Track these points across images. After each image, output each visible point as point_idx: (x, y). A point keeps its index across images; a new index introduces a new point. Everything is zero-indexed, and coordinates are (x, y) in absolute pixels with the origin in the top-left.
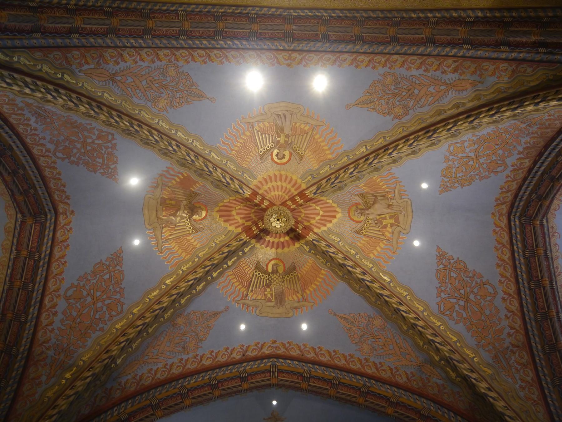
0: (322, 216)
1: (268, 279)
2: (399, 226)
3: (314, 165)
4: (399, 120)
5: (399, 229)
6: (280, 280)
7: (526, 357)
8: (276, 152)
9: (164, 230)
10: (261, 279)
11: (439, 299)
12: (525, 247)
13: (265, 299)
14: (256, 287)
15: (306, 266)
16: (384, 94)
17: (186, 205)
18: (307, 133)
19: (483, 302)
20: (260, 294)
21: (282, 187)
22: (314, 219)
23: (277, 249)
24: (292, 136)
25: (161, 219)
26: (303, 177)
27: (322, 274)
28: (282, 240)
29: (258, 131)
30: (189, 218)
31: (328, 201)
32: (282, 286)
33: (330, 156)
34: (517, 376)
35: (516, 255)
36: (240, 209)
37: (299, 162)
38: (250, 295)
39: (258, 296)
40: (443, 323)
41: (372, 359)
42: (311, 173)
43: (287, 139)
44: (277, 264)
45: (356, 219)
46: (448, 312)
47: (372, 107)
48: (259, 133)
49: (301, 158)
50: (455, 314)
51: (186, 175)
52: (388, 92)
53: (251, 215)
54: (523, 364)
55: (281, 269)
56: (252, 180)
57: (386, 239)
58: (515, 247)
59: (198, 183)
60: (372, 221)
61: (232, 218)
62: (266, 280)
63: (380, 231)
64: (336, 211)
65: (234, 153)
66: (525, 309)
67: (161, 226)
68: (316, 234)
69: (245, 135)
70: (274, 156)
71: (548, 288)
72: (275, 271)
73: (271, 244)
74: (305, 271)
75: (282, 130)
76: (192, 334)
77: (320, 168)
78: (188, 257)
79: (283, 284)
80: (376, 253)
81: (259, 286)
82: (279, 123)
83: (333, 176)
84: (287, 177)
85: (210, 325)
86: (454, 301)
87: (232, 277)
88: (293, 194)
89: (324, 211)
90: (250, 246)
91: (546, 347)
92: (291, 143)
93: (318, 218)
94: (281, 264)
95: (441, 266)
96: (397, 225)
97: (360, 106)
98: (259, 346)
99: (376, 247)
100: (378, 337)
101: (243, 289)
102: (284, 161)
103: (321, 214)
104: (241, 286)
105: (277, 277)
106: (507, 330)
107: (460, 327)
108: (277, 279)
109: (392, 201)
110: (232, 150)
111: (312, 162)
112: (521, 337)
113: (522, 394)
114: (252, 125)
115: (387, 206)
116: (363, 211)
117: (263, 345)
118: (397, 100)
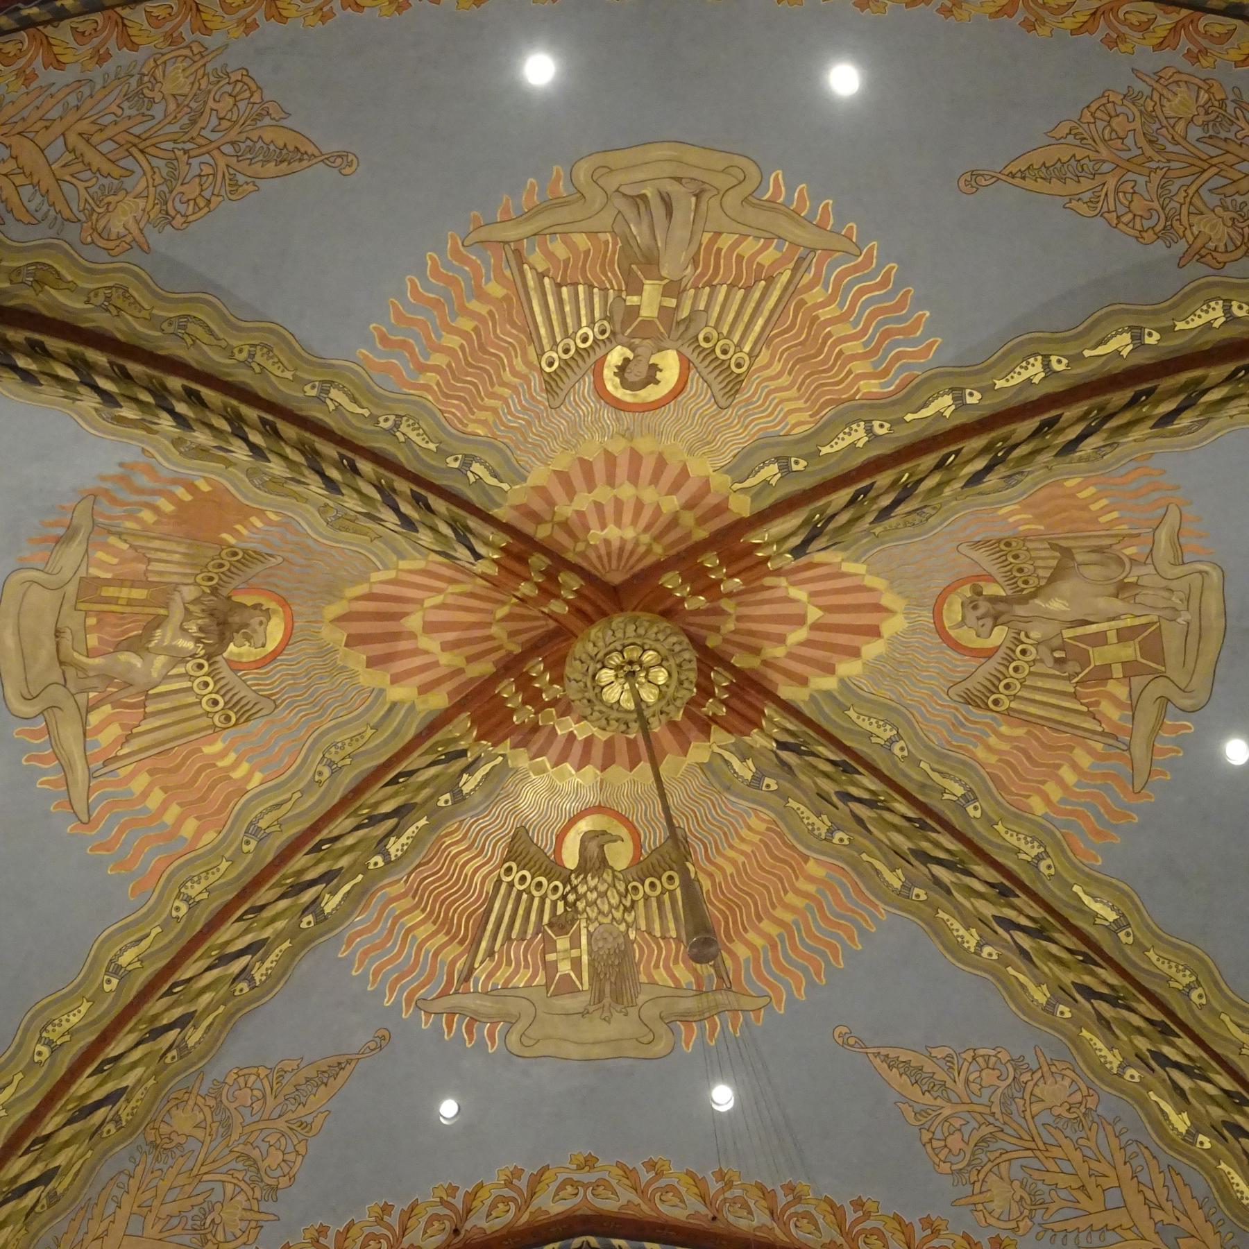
0: (816, 627)
1: (564, 897)
3: (792, 419)
4: (1212, 271)
5: (1159, 688)
6: (615, 901)
8: (616, 356)
9: (94, 719)
10: (532, 898)
13: (547, 986)
14: (508, 938)
15: (736, 842)
16: (1149, 152)
17: (196, 601)
18: (770, 280)
20: (527, 966)
21: (639, 506)
22: (781, 639)
23: (603, 768)
24: (697, 288)
25: (78, 667)
26: (741, 466)
27: (811, 879)
29: (541, 276)
30: (208, 657)
31: (848, 567)
32: (623, 927)
33: (871, 387)
36: (443, 606)
37: (723, 403)
38: (481, 972)
39: (516, 971)
42: (778, 451)
43: (672, 303)
44: (604, 833)
45: (967, 637)
47: (1087, 196)
48: (546, 280)
49: (734, 384)
51: (205, 487)
52: (1170, 147)
53: (494, 630)
55: (620, 856)
56: (505, 486)
57: (1103, 734)
59: (261, 513)
60: (1042, 648)
61: (403, 645)
62: (554, 904)
63: (1075, 696)
64: (878, 608)
65: (431, 378)
67: (82, 699)
68: (788, 708)
69: (480, 295)
70: (608, 373)
72: (594, 863)
73: (577, 750)
74: (734, 862)
75: (651, 262)
76: (234, 1165)
77: (824, 432)
78: (209, 837)
79: (630, 918)
80: (1055, 793)
81: (524, 931)
82: (639, 231)
83: (883, 479)
84: (661, 464)
85: (309, 1119)
87: (407, 903)
88: (689, 534)
89: (827, 609)
90: (488, 767)
92: (690, 319)
93: (797, 635)
94: (623, 832)
96: (1151, 671)
97: (1029, 183)
98: (523, 1184)
99: (1058, 767)
100: (1056, 1152)
101: (453, 951)
102: (651, 393)
103: (810, 620)
104: (442, 938)
105: (602, 888)
108: (603, 895)
109: (1137, 571)
110: (423, 369)
111: (788, 406)
114: (518, 253)
115: (1112, 589)
116: (1001, 607)
117: (536, 1180)
118: (1210, 185)
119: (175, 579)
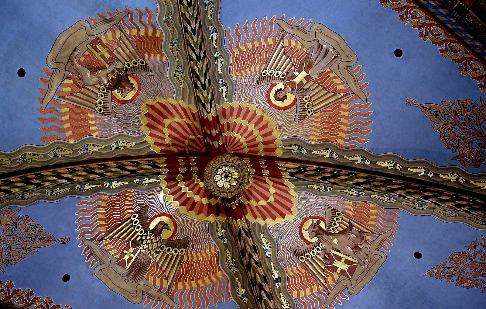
0: (269, 203)
1: (142, 236)
2: (349, 279)
3: (312, 137)
4: (461, 165)
5: (347, 282)
6: (154, 247)
8: (280, 86)
9: (66, 81)
10: (134, 230)
13: (118, 260)
14: (119, 237)
15: (203, 252)
16: (467, 123)
17: (119, 70)
18: (336, 94)
20: (117, 250)
21: (251, 133)
22: (258, 201)
23: (180, 205)
24: (315, 83)
25: (73, 63)
26: (286, 142)
27: (216, 277)
28: (197, 198)
29: (283, 47)
30: (108, 89)
31: (292, 192)
32: (151, 257)
33: (340, 141)
36: (179, 124)
37: (296, 120)
38: (105, 242)
39: (113, 249)
42: (301, 144)
43: (305, 82)
44: (166, 225)
45: (306, 234)
47: (440, 125)
48: (283, 49)
49: (304, 117)
51: (158, 35)
52: (474, 125)
53: (186, 141)
55: (166, 235)
56: (226, 100)
57: (324, 286)
59: (162, 56)
60: (323, 251)
61: (160, 127)
62: (138, 236)
63: (323, 270)
64: (289, 210)
65: (237, 52)
67: (67, 73)
68: (247, 222)
69: (266, 39)
70: (274, 89)
72: (157, 232)
73: (179, 194)
74: (198, 258)
75: (309, 66)
76: (5, 245)
77: (318, 147)
78: (72, 140)
79: (155, 256)
81: (124, 238)
83: (328, 169)
84: (266, 126)
85: (32, 249)
87: (104, 204)
88: (258, 152)
89: (275, 200)
90: (154, 180)
92: (306, 90)
93: (263, 203)
94: (172, 228)
96: (348, 277)
97: (426, 112)
99: (307, 287)
101: (103, 229)
102: (279, 104)
103: (269, 201)
104: (103, 223)
105: (154, 241)
108: (152, 243)
109: (364, 245)
110: (238, 47)
111: (314, 133)
114: (284, 35)
115: (353, 246)
116: (321, 232)
118: (477, 141)
119: (120, 57)
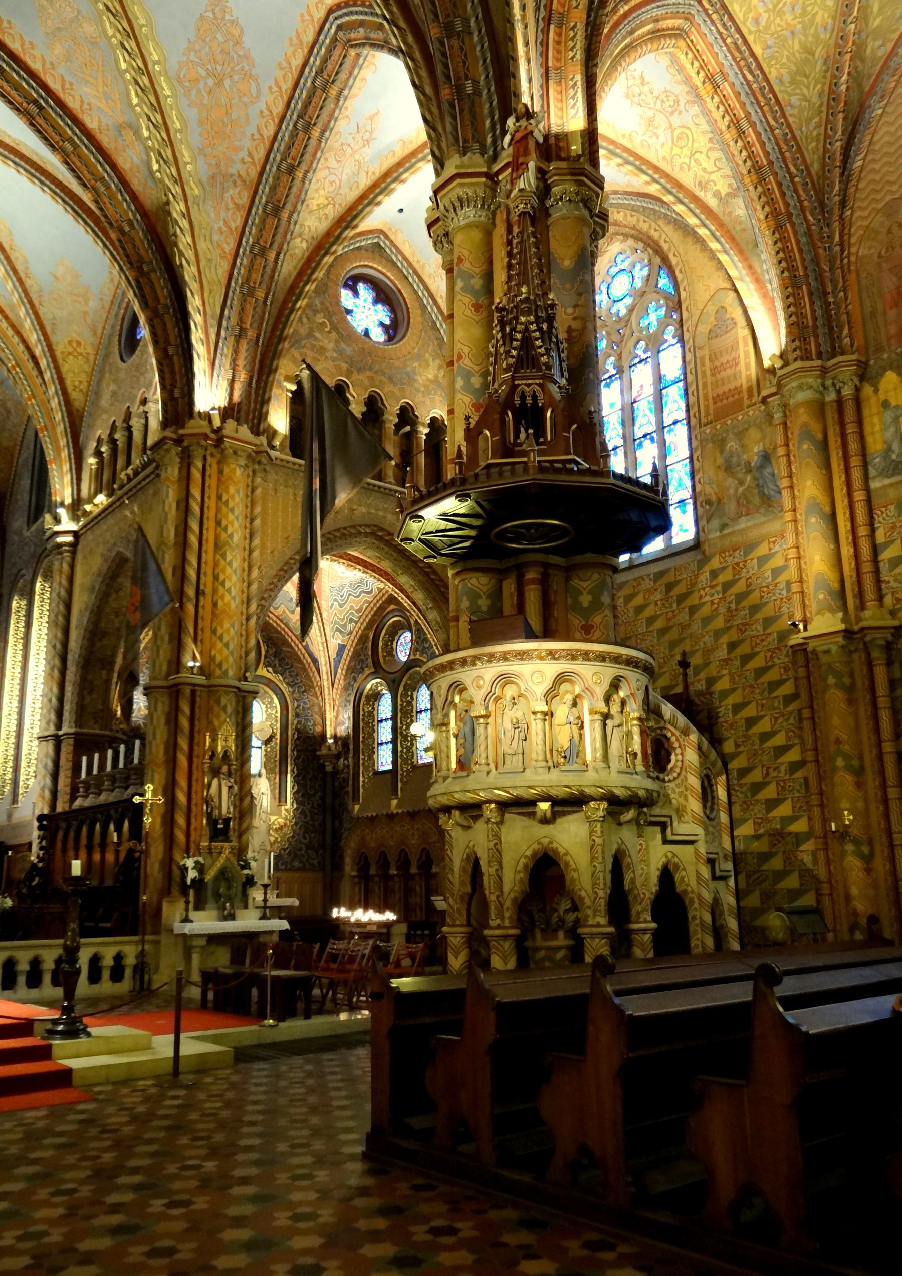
7: (245, 200)
11: (185, 58)
12: (320, 72)
19: (236, 99)
34: (223, 214)
35: (307, 70)
40: (175, 96)
41: (61, 70)
46: (187, 84)
50: (194, 92)
54: (237, 205)
58: (312, 59)
66: (276, 145)
71: (313, 142)
86: (204, 73)
91: (270, 206)
95: (210, 14)
106: (244, 154)
107: (192, 114)
112: (254, 173)
113: (216, 237)
